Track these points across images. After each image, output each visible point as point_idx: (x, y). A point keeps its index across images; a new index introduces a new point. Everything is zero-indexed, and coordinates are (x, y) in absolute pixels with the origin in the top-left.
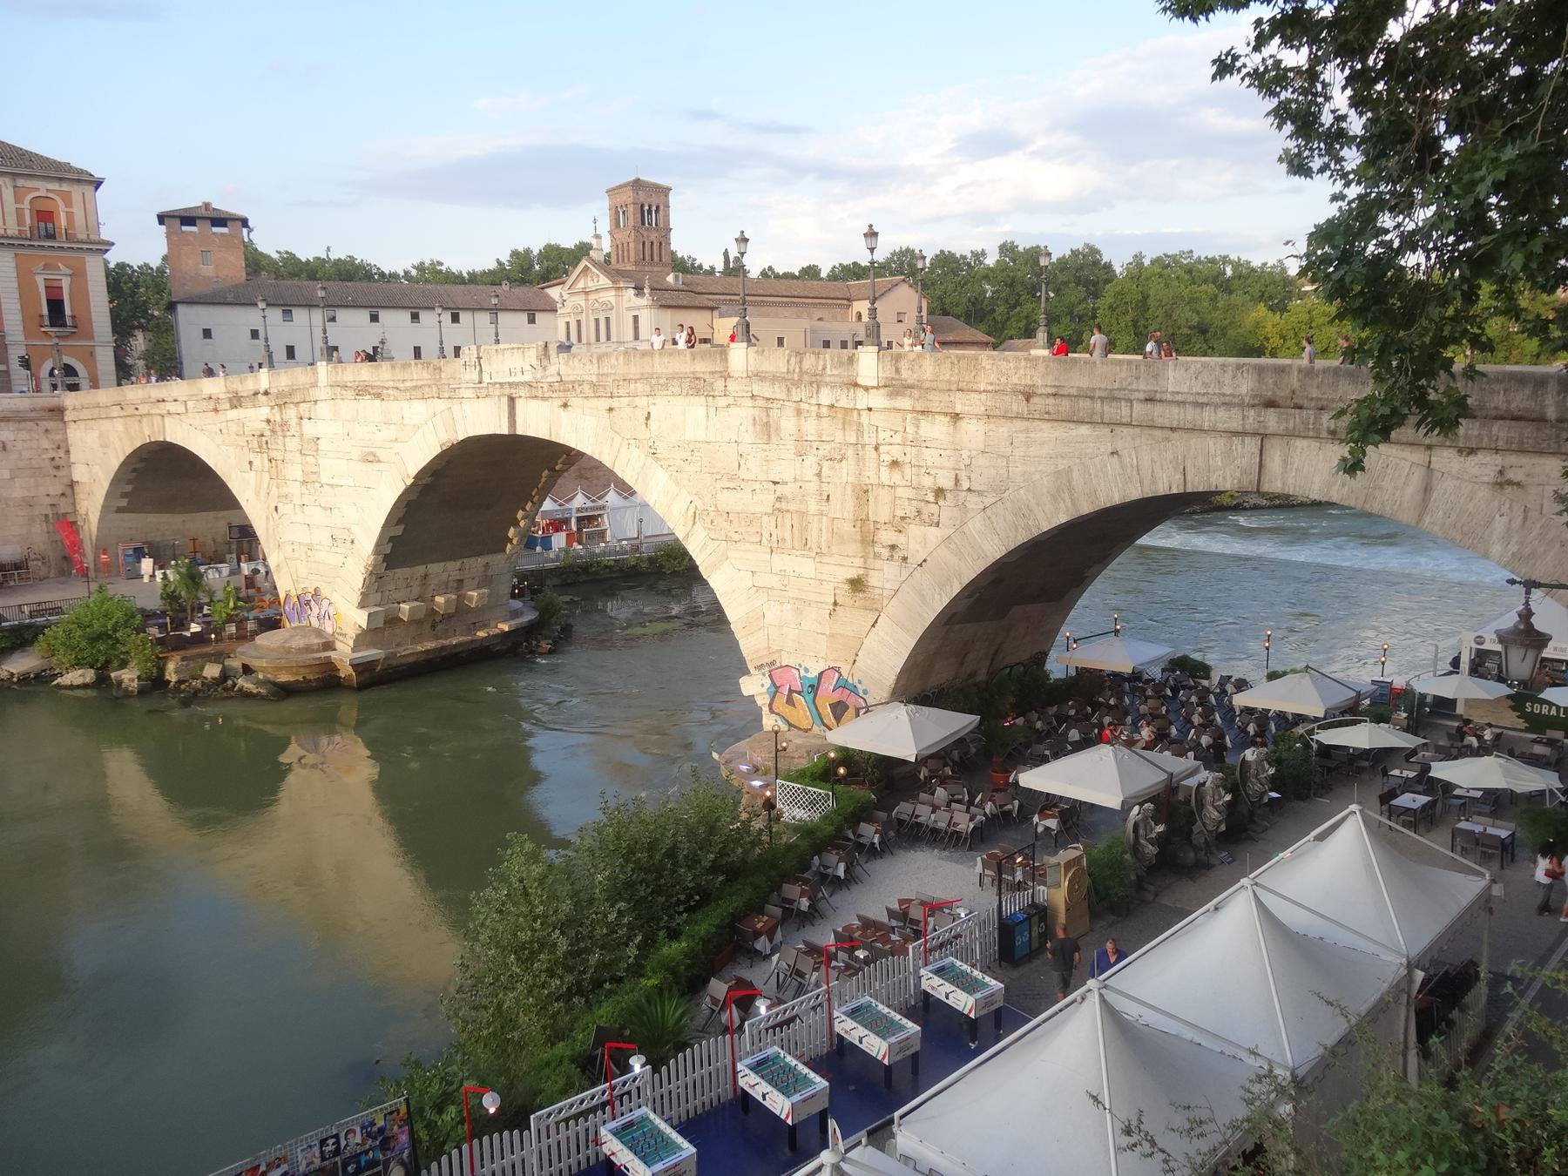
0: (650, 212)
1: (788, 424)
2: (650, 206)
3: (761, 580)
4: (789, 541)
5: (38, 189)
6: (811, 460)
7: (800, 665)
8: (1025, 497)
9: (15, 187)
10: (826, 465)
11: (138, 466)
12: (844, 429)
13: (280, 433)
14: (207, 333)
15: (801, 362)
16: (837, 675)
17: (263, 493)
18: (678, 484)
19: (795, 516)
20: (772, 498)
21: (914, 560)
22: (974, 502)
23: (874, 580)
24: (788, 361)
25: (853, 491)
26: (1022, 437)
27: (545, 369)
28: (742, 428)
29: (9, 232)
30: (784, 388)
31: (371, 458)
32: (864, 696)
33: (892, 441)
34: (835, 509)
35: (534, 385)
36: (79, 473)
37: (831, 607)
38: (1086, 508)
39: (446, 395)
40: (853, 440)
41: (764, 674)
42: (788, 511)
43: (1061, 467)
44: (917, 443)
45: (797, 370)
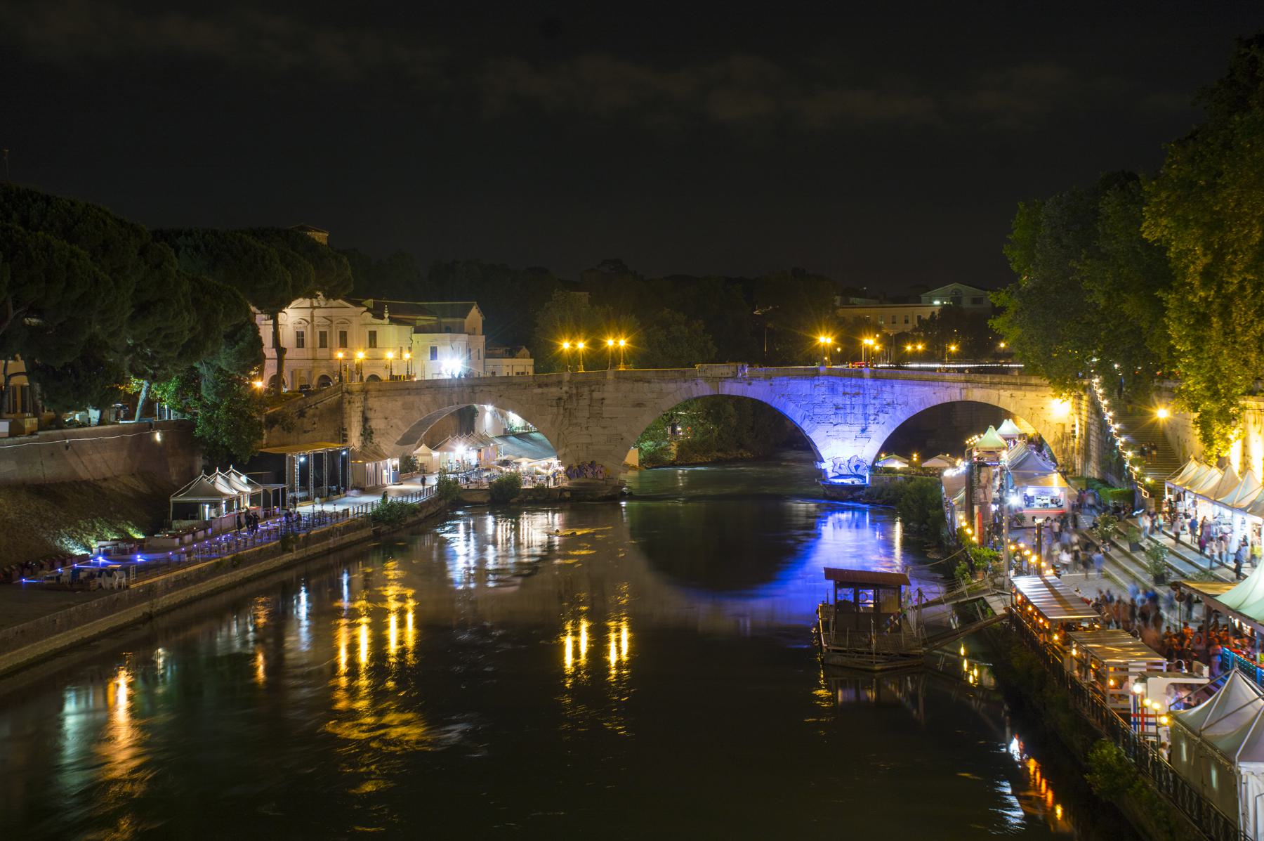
38: (928, 407)
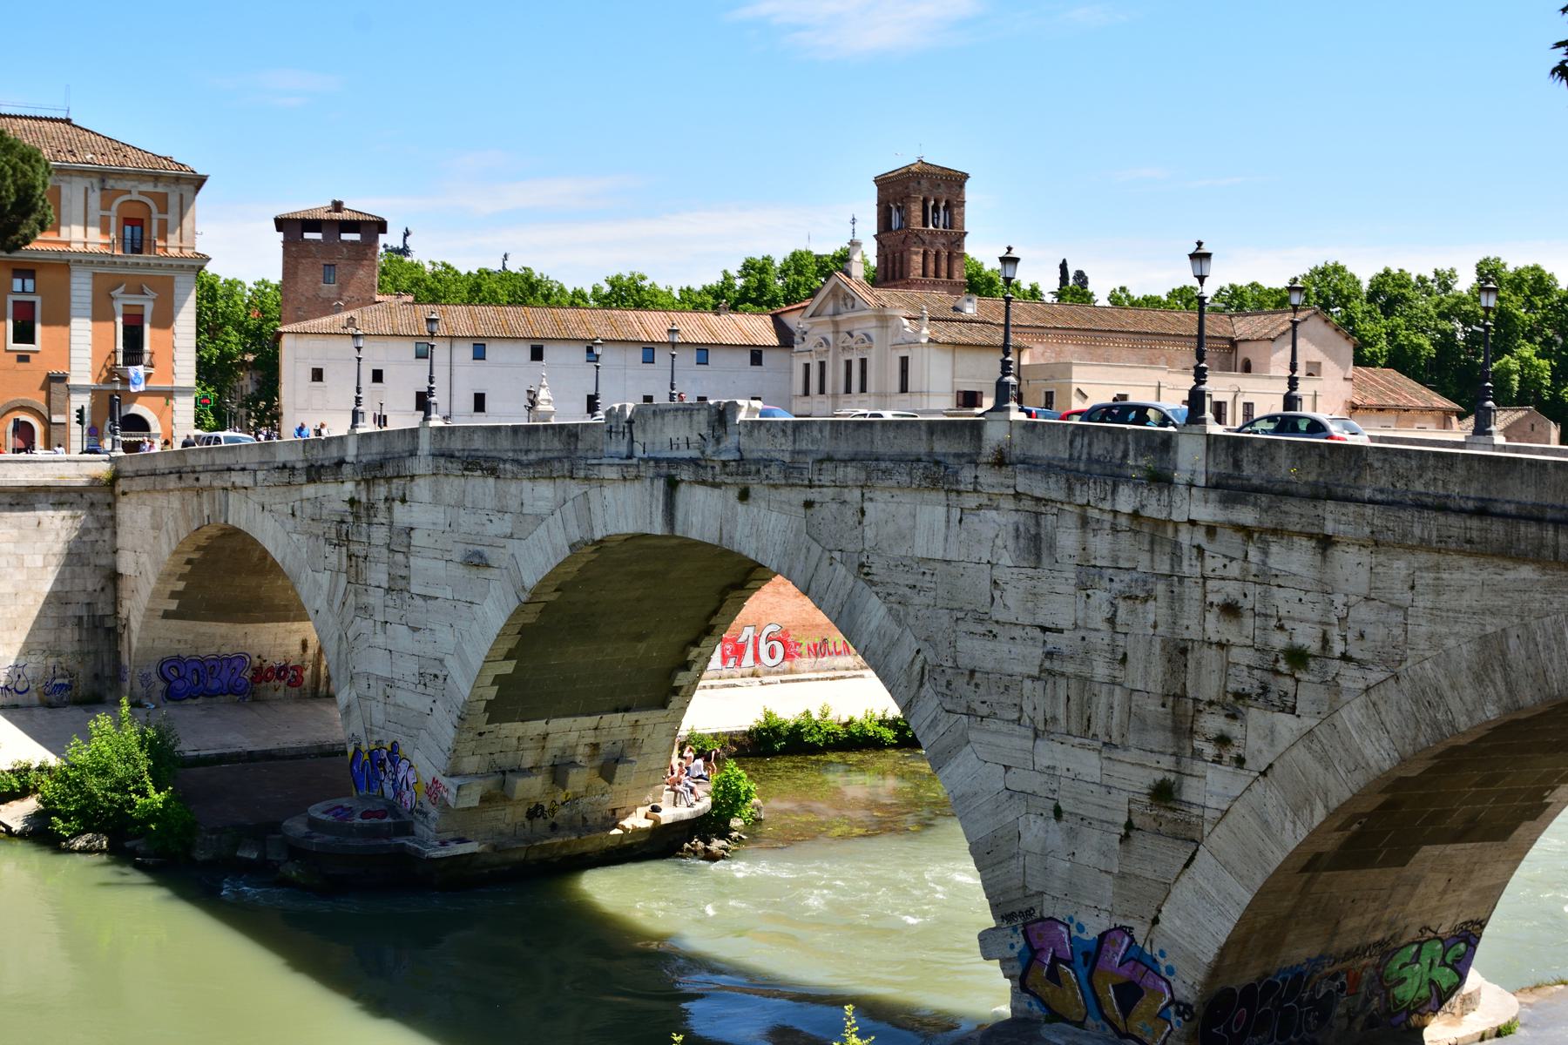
0: (936, 209)
1: (1068, 539)
2: (937, 202)
3: (1019, 780)
4: (1063, 722)
5: (129, 192)
6: (1100, 597)
7: (1071, 919)
8: (1431, 675)
9: (103, 189)
10: (1123, 607)
11: (195, 556)
12: (1152, 551)
13: (364, 520)
14: (318, 375)
15: (1090, 445)
16: (1127, 940)
17: (337, 602)
18: (899, 622)
19: (1073, 683)
20: (1039, 652)
21: (1255, 764)
22: (1351, 678)
23: (1191, 791)
24: (1071, 443)
25: (1163, 649)
26: (1428, 577)
27: (718, 441)
28: (999, 542)
30: (1063, 483)
31: (476, 561)
32: (1167, 977)
33: (1225, 573)
34: (1134, 676)
35: (703, 463)
36: (126, 564)
37: (1123, 831)
39: (582, 474)
40: (1164, 568)
41: (1015, 929)
42: (1063, 674)
43: (1490, 629)
44: (1265, 578)
45: (1084, 457)
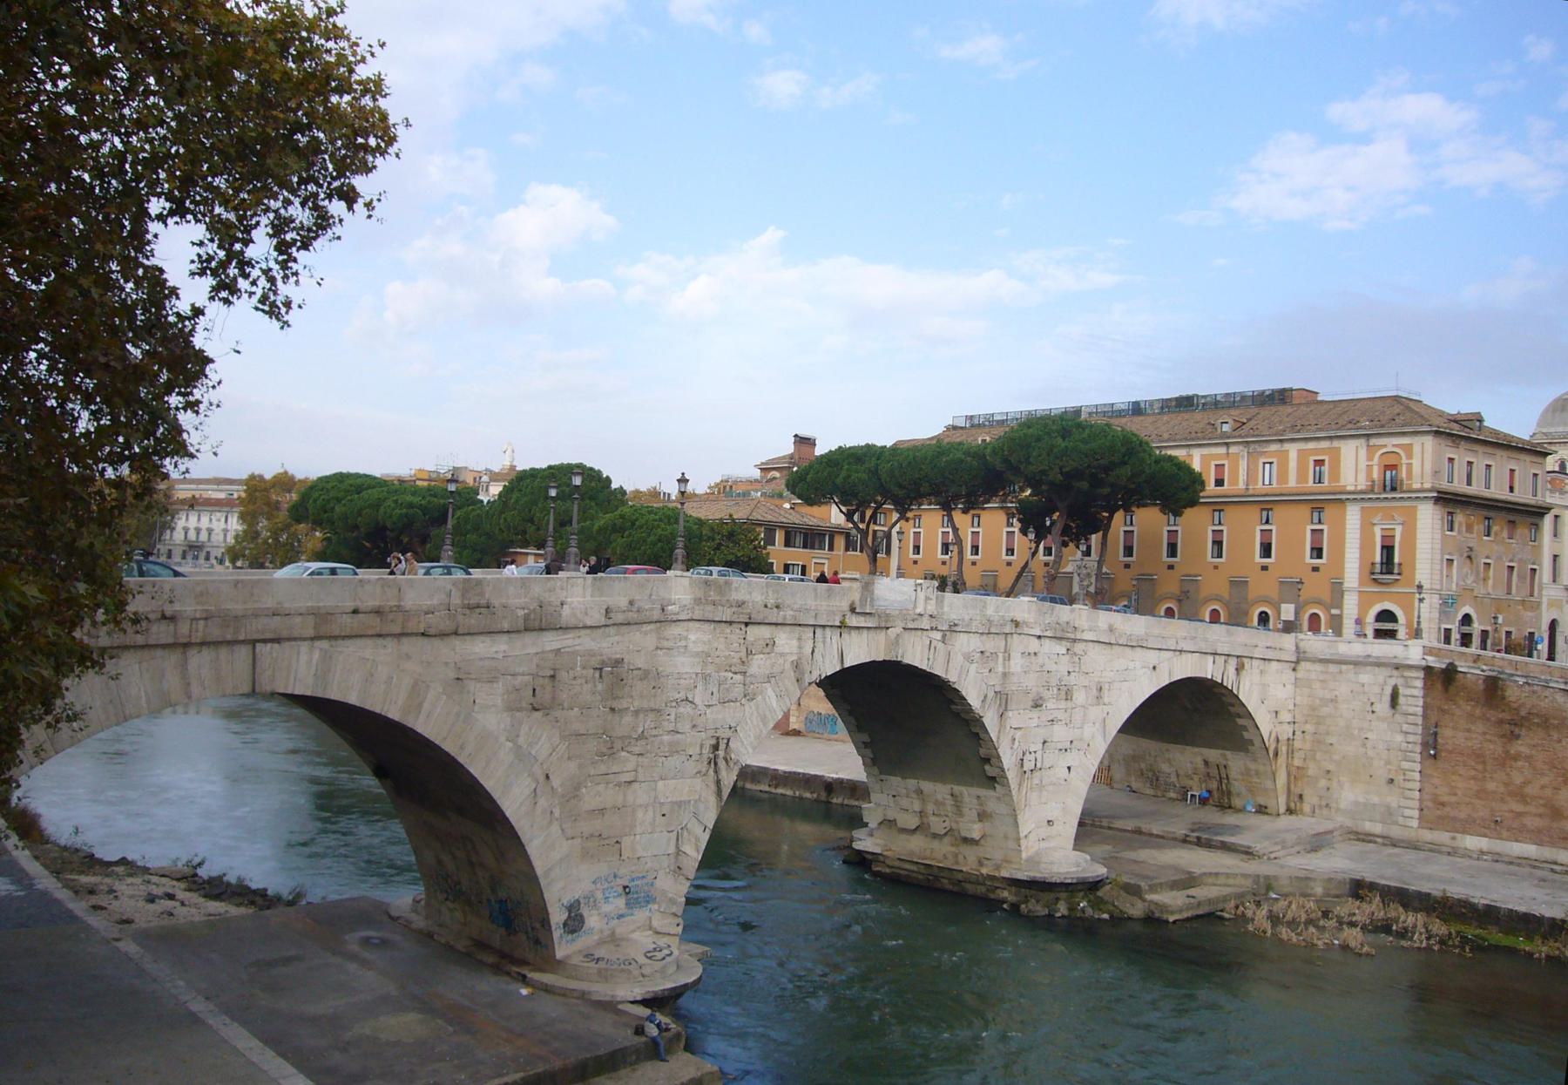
5: (1385, 446)
9: (1368, 446)
29: (1359, 488)
